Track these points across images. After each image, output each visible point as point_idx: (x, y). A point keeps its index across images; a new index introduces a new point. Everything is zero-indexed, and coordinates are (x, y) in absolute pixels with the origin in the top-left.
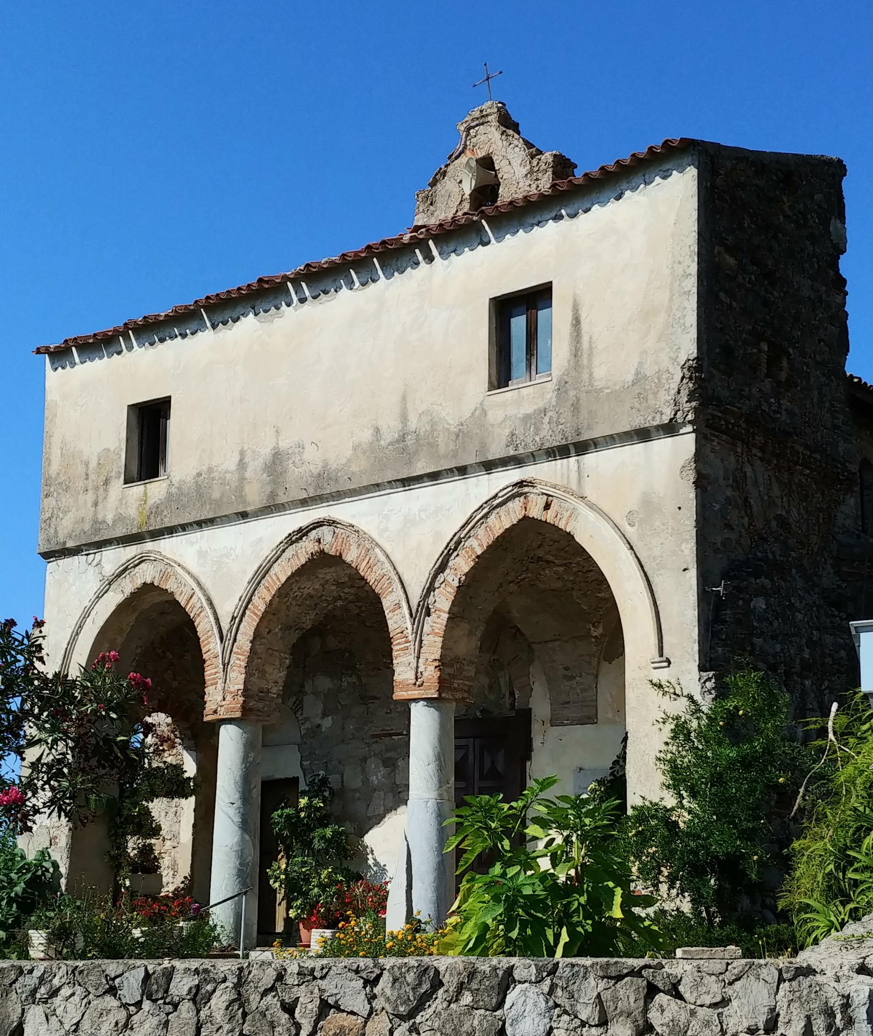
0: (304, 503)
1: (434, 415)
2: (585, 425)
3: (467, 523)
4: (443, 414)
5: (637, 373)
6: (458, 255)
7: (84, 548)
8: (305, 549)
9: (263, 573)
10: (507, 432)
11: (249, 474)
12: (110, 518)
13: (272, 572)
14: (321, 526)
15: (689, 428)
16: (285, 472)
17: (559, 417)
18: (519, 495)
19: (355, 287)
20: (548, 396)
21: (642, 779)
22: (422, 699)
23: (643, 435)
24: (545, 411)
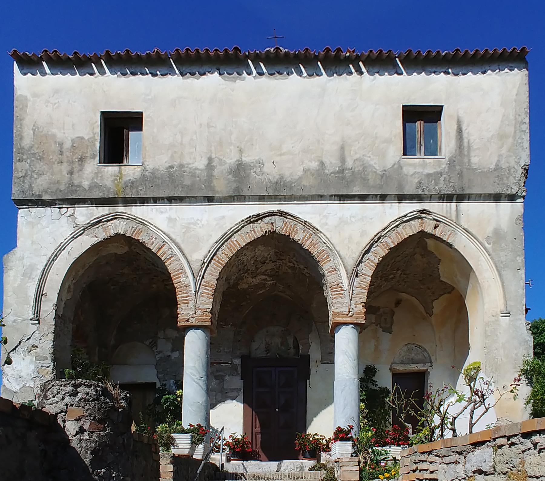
0: (262, 199)
1: (365, 162)
2: (467, 186)
3: (386, 228)
4: (372, 163)
5: (497, 165)
6: (380, 75)
7: (57, 202)
8: (260, 229)
9: (227, 238)
10: (416, 180)
11: (216, 173)
12: (86, 184)
13: (233, 238)
14: (274, 215)
15: (522, 200)
16: (248, 176)
17: (450, 178)
18: (418, 218)
19: (303, 76)
20: (443, 166)
21: (494, 370)
22: (352, 324)
23: (497, 198)
24: (441, 174)
